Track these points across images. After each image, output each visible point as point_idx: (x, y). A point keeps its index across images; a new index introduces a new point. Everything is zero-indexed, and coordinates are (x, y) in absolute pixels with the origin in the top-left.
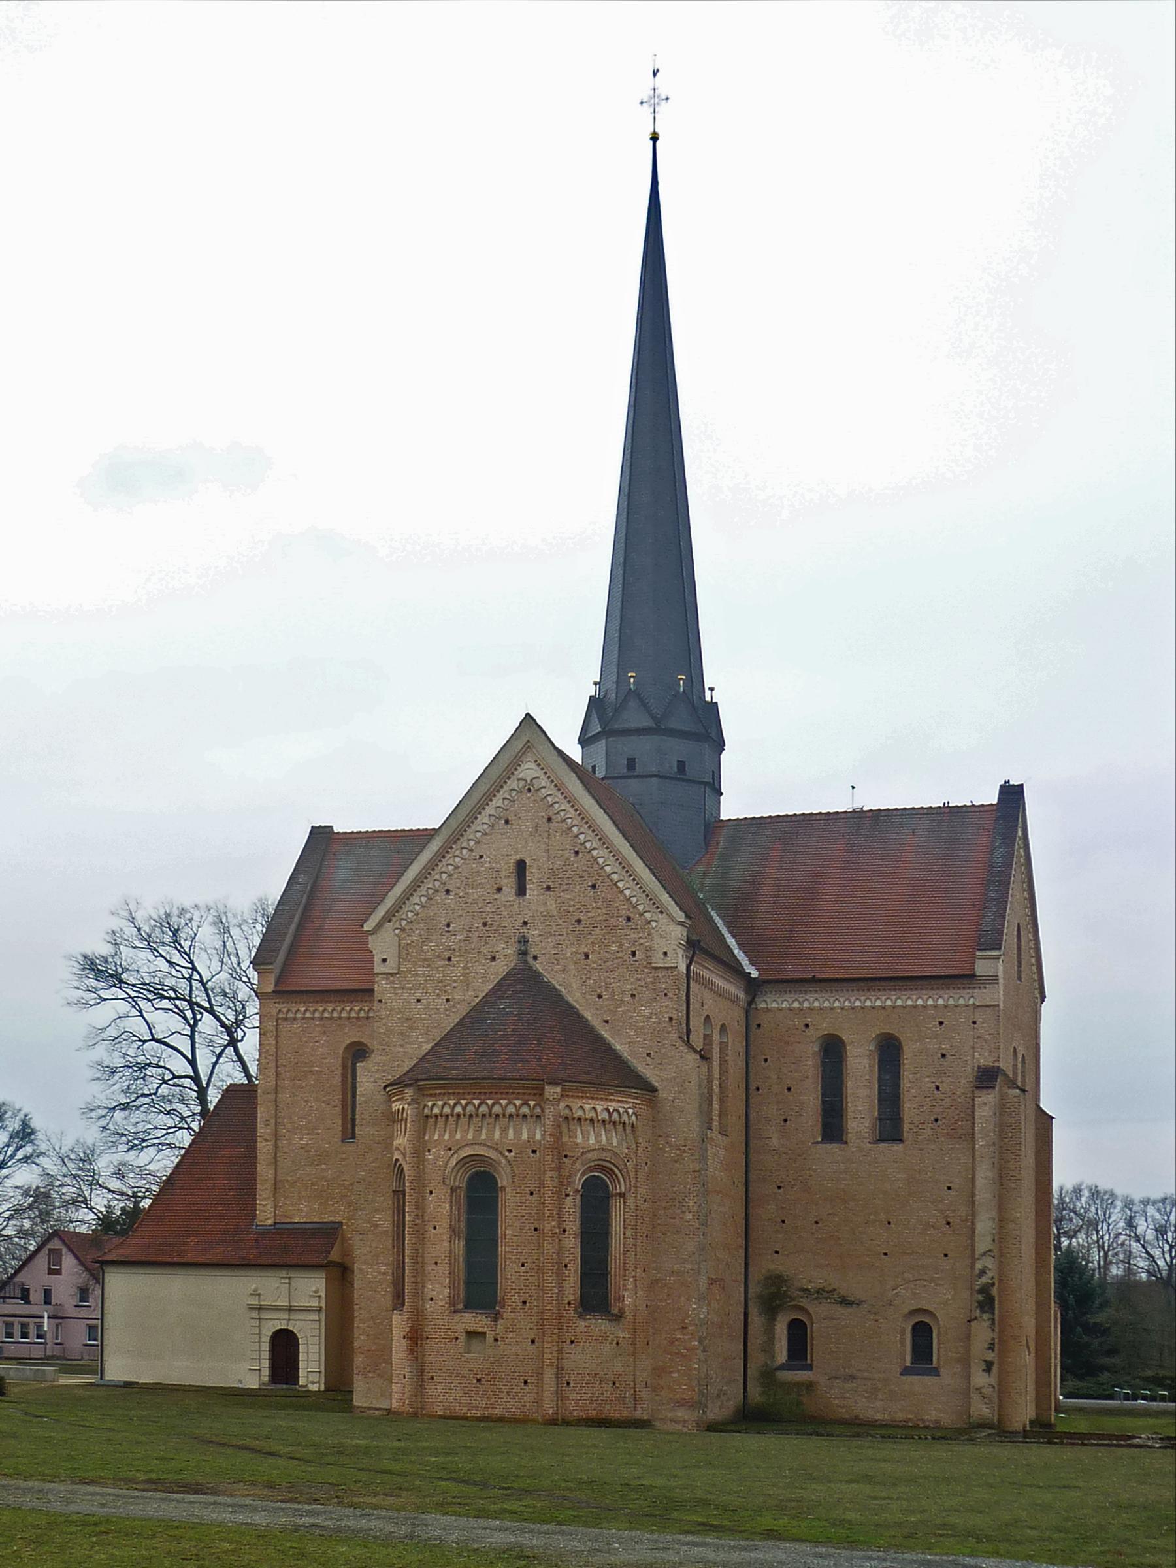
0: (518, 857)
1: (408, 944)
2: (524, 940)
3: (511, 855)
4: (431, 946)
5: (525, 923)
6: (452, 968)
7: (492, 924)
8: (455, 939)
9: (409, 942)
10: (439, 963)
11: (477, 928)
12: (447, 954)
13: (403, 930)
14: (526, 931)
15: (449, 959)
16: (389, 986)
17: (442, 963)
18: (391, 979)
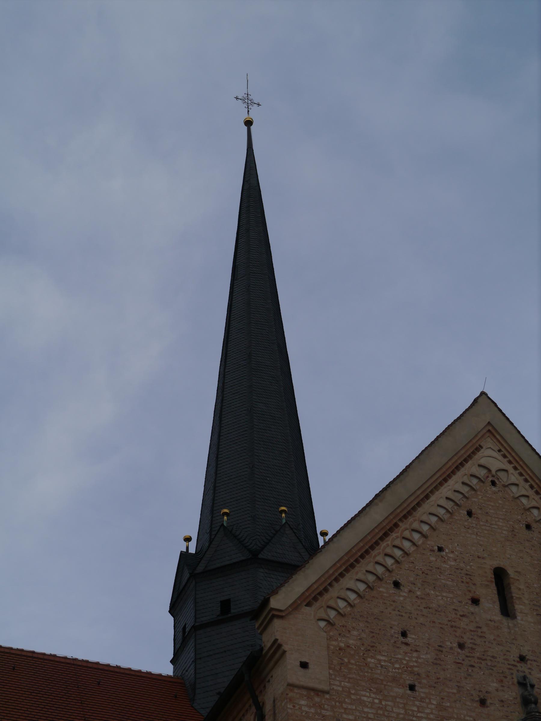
0: (496, 563)
1: (340, 649)
2: (523, 683)
3: (483, 558)
4: (380, 660)
5: (522, 659)
6: (417, 703)
7: (472, 649)
8: (419, 657)
9: (342, 645)
10: (396, 690)
11: (451, 648)
12: (409, 680)
13: (330, 623)
14: (527, 671)
15: (412, 688)
16: (313, 710)
17: (400, 691)
18: (317, 699)
